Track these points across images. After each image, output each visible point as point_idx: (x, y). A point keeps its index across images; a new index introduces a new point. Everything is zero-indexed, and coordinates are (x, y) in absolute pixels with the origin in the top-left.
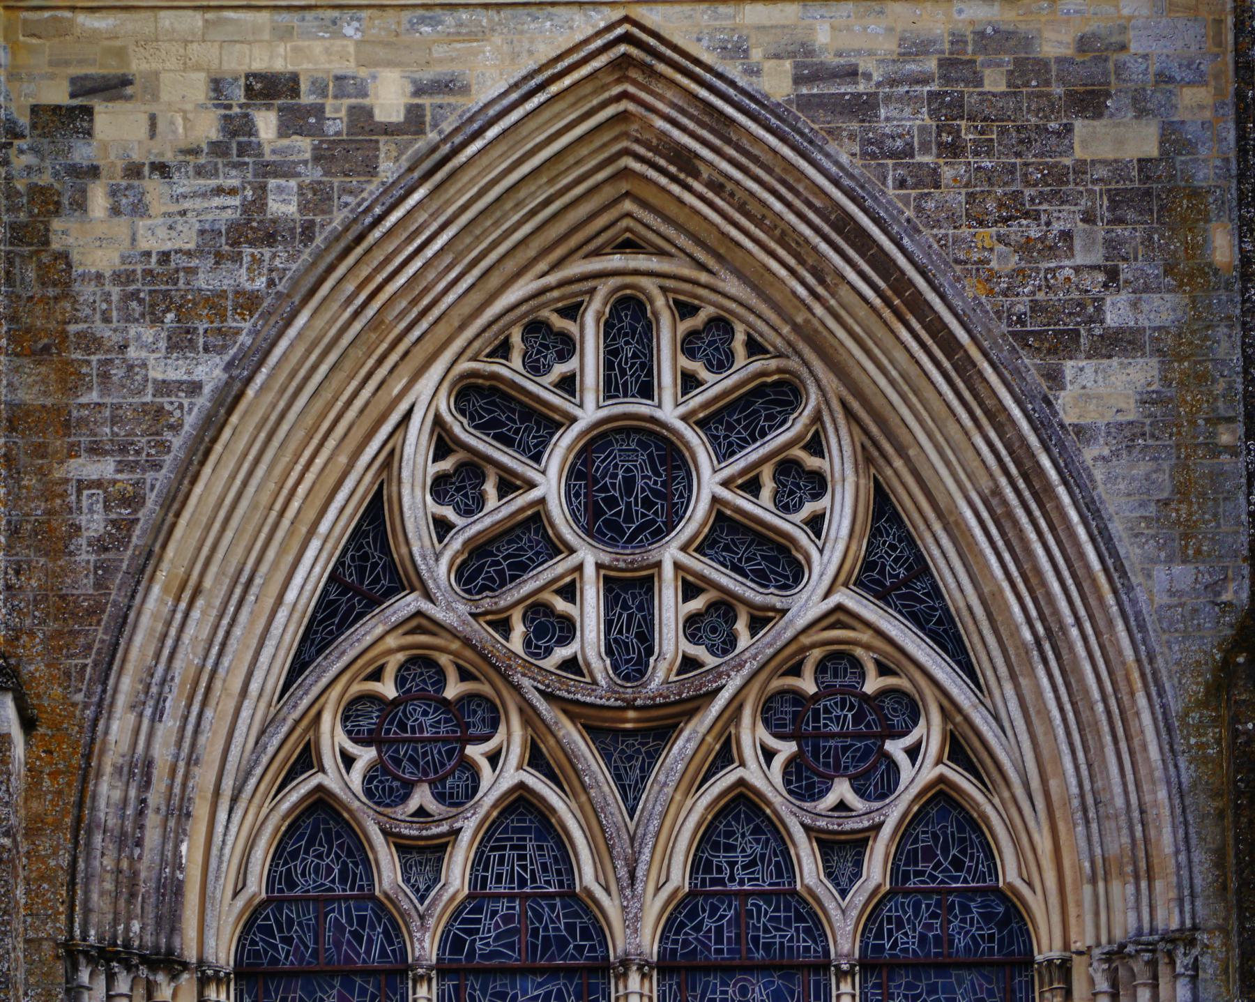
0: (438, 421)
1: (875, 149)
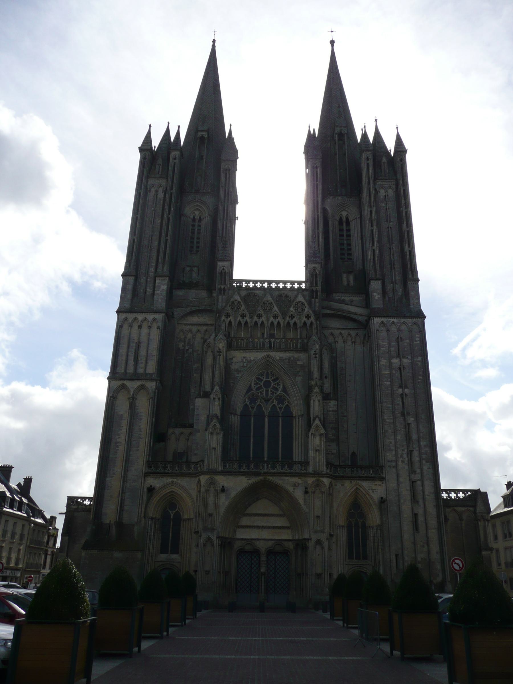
0: (255, 380)
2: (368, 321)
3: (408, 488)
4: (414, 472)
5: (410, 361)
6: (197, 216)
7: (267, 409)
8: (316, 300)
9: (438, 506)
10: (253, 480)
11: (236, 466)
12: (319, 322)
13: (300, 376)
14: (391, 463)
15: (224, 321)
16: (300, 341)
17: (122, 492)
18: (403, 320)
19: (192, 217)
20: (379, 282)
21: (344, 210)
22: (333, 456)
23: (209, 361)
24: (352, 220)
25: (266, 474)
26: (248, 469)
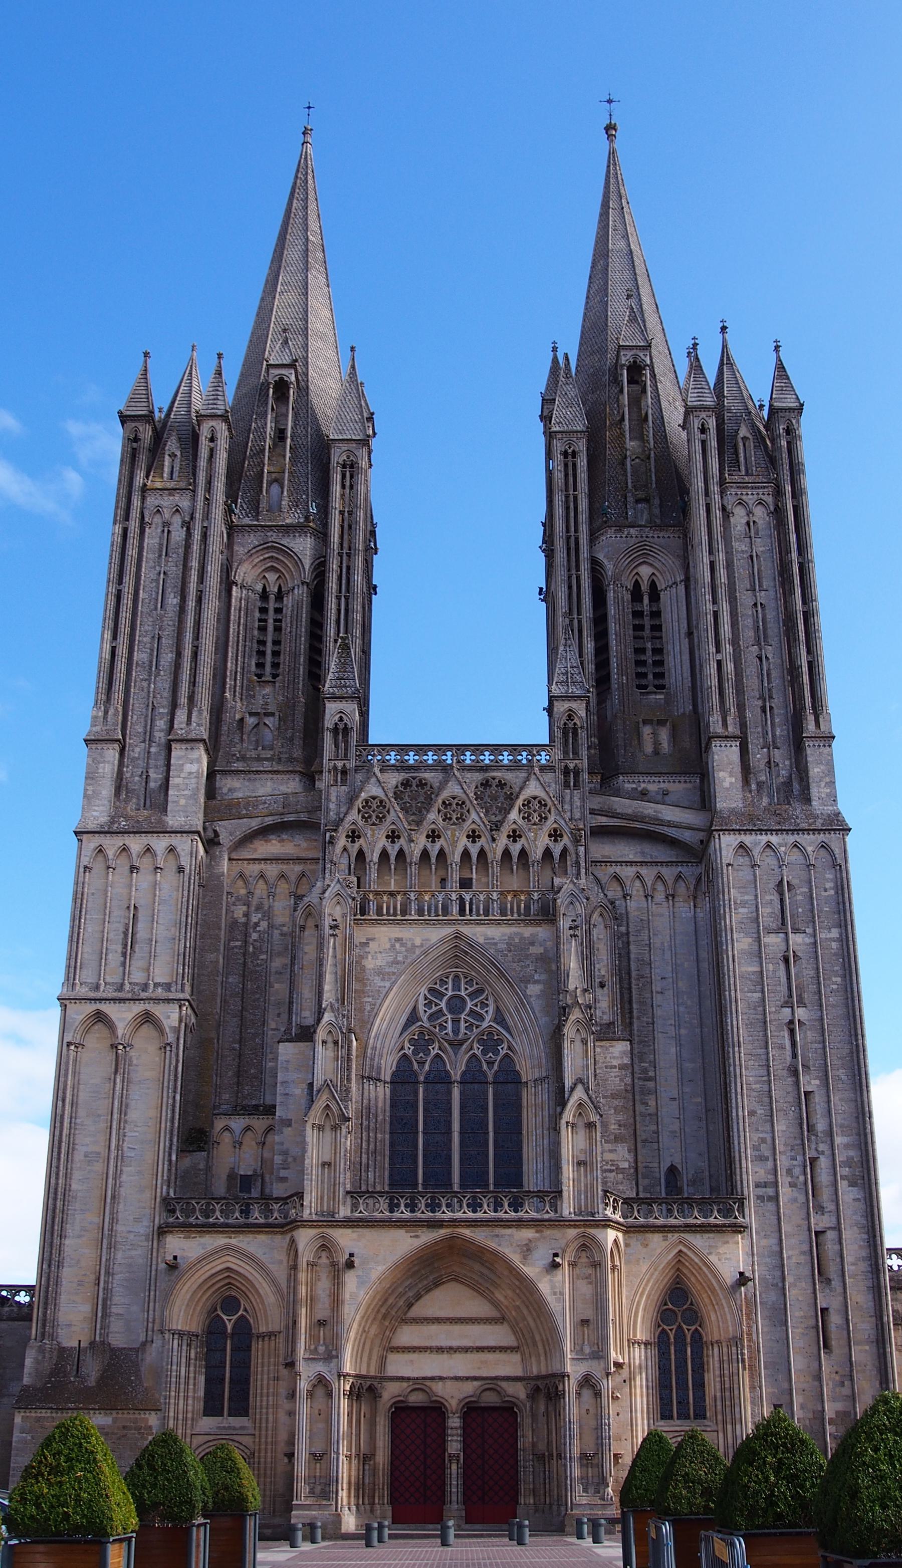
1: (497, 951)
2: (705, 844)
3: (806, 1247)
4: (820, 1209)
5: (809, 940)
6: (272, 585)
7: (457, 1068)
8: (575, 792)
9: (877, 1291)
10: (427, 1237)
11: (383, 1204)
12: (582, 849)
13: (537, 982)
14: (764, 1189)
15: (345, 849)
16: (536, 896)
17: (108, 1273)
18: (791, 839)
19: (259, 587)
20: (733, 744)
21: (644, 562)
22: (621, 1176)
23: (309, 950)
24: (666, 588)
25: (454, 1223)
26: (412, 1211)
